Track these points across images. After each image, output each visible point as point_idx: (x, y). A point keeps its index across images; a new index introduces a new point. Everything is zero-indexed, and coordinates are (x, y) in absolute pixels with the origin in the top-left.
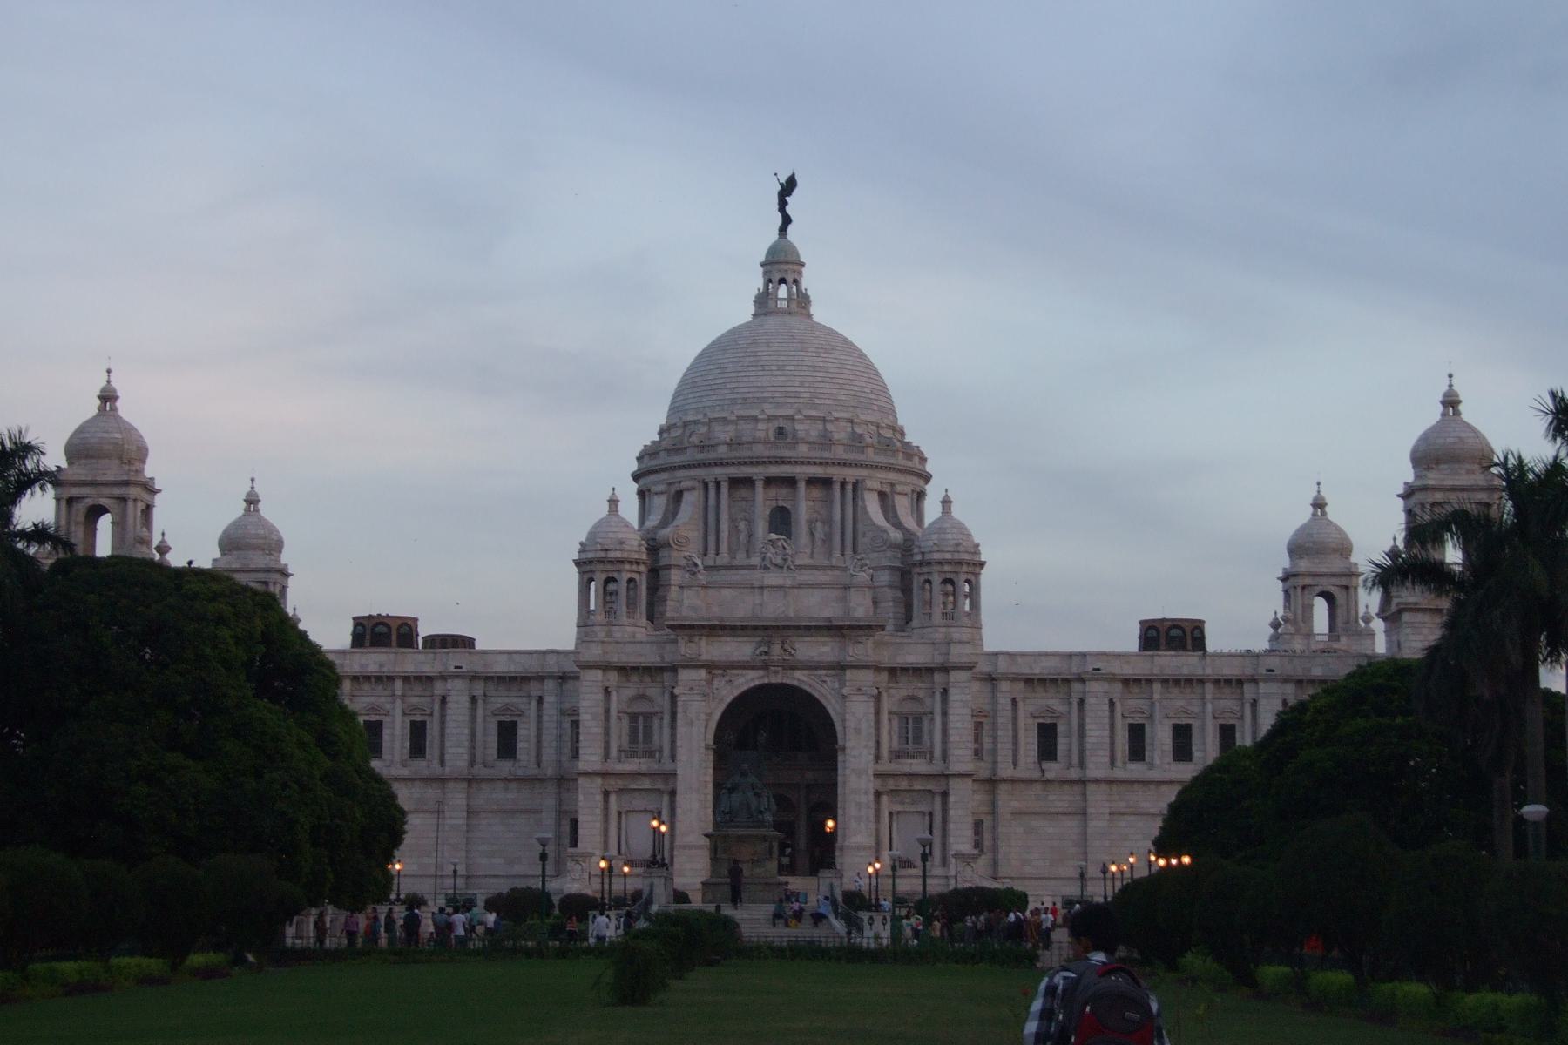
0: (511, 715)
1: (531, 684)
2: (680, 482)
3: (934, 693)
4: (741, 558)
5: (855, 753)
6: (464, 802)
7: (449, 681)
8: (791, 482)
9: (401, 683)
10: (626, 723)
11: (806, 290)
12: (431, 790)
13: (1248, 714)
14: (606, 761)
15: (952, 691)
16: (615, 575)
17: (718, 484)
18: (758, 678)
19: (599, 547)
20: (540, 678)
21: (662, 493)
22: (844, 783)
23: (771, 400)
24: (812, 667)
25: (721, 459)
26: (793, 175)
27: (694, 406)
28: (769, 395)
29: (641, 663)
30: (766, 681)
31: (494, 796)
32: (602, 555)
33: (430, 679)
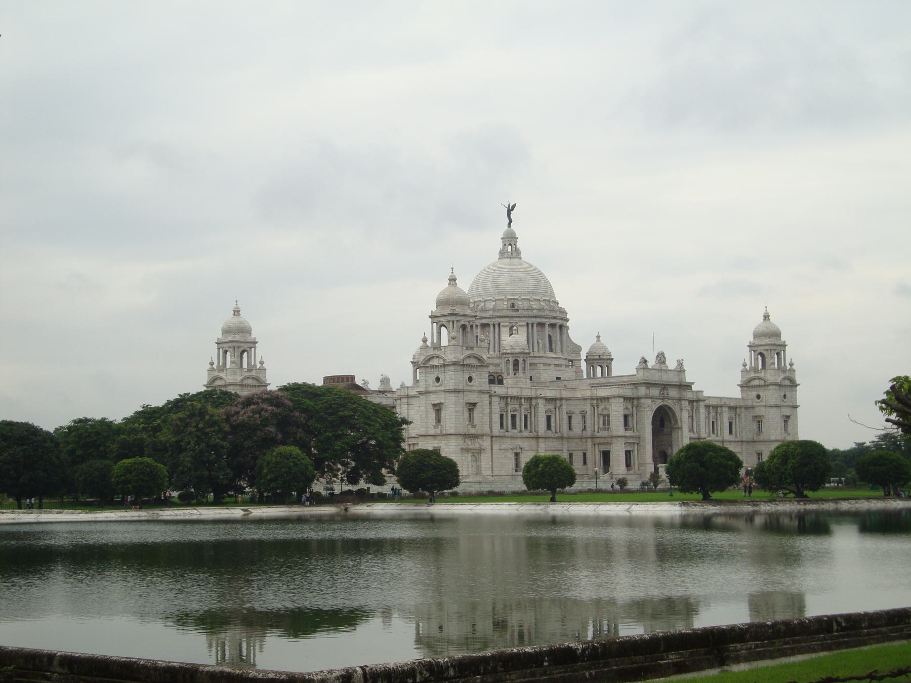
2: (517, 323)
3: (692, 410)
4: (542, 354)
8: (552, 326)
12: (533, 442)
13: (719, 418)
15: (701, 409)
16: (525, 359)
17: (532, 325)
19: (521, 347)
20: (561, 399)
21: (507, 326)
26: (516, 204)
28: (540, 291)
32: (522, 351)
33: (531, 399)
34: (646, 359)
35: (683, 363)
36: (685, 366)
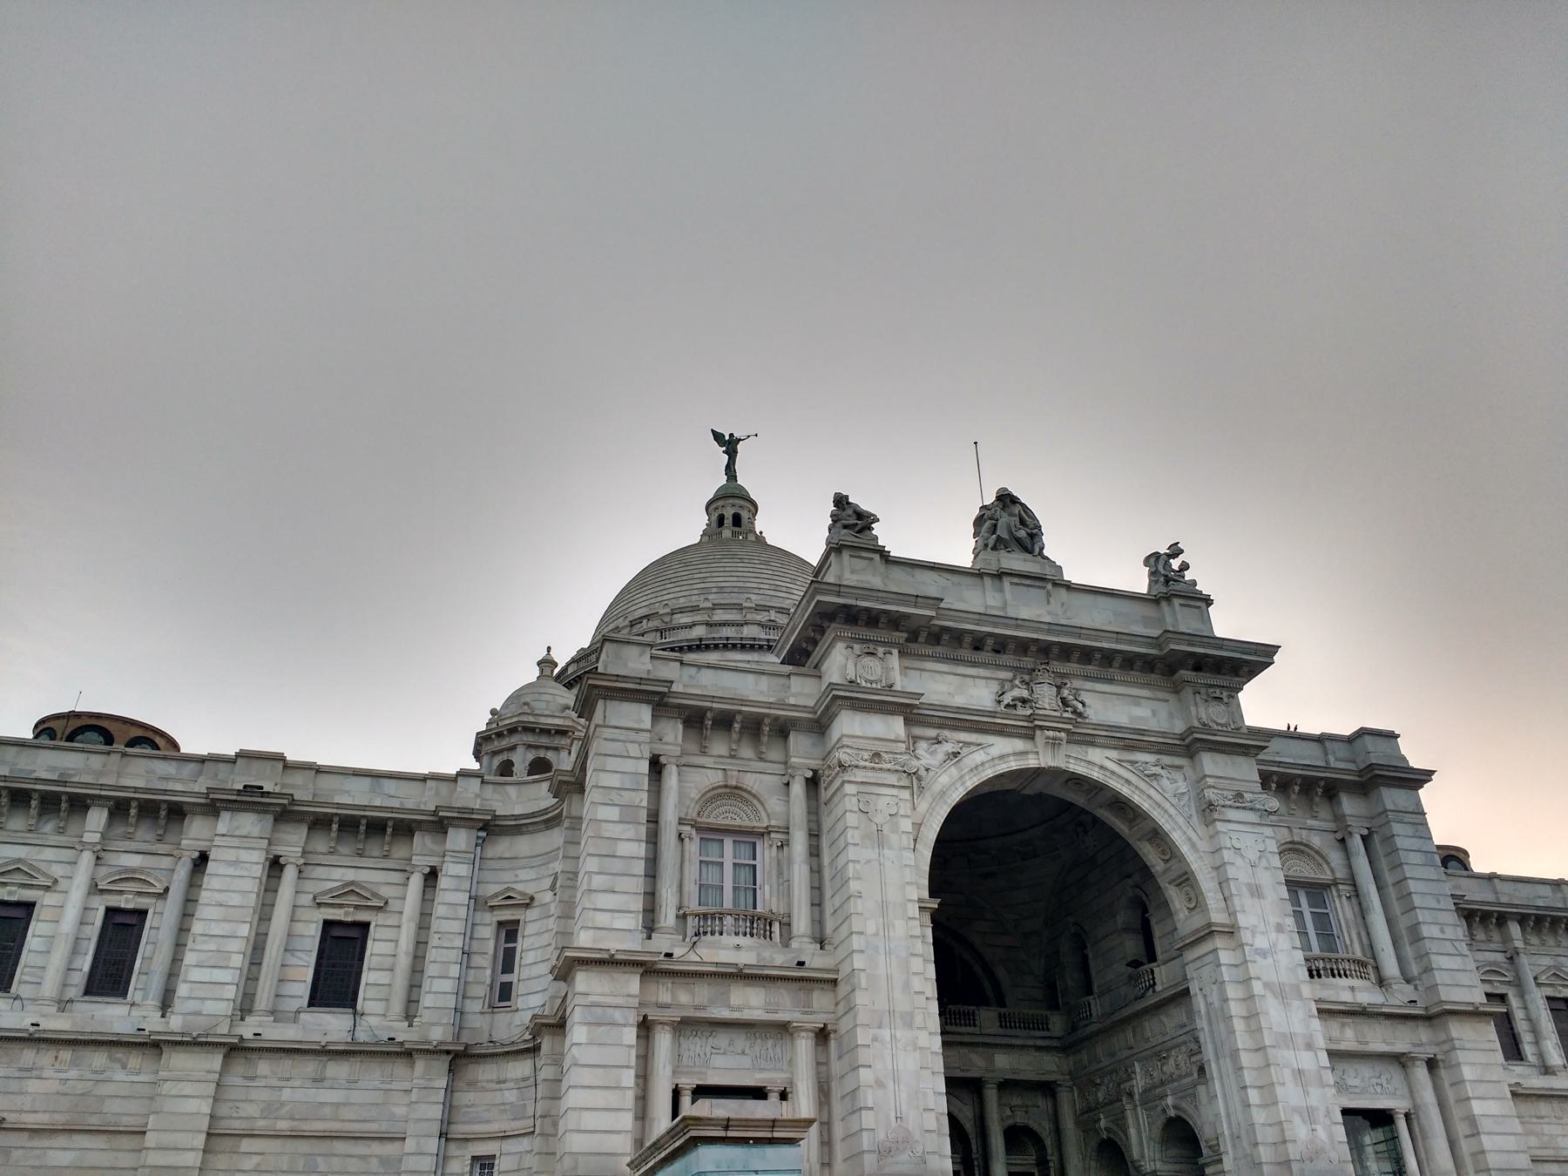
0: (357, 907)
1: (417, 837)
3: (1343, 841)
5: (1261, 942)
6: (206, 1108)
7: (225, 816)
9: (105, 813)
10: (693, 847)
11: (761, 533)
12: (120, 1075)
14: (649, 938)
15: (1397, 828)
16: (550, 755)
18: (1015, 754)
20: (439, 824)
22: (1252, 1017)
23: (756, 591)
24: (1128, 741)
25: (701, 640)
27: (646, 603)
29: (744, 702)
30: (1032, 762)
31: (286, 1094)
32: (531, 719)
33: (177, 813)
34: (865, 506)
35: (1185, 567)
36: (1202, 577)
